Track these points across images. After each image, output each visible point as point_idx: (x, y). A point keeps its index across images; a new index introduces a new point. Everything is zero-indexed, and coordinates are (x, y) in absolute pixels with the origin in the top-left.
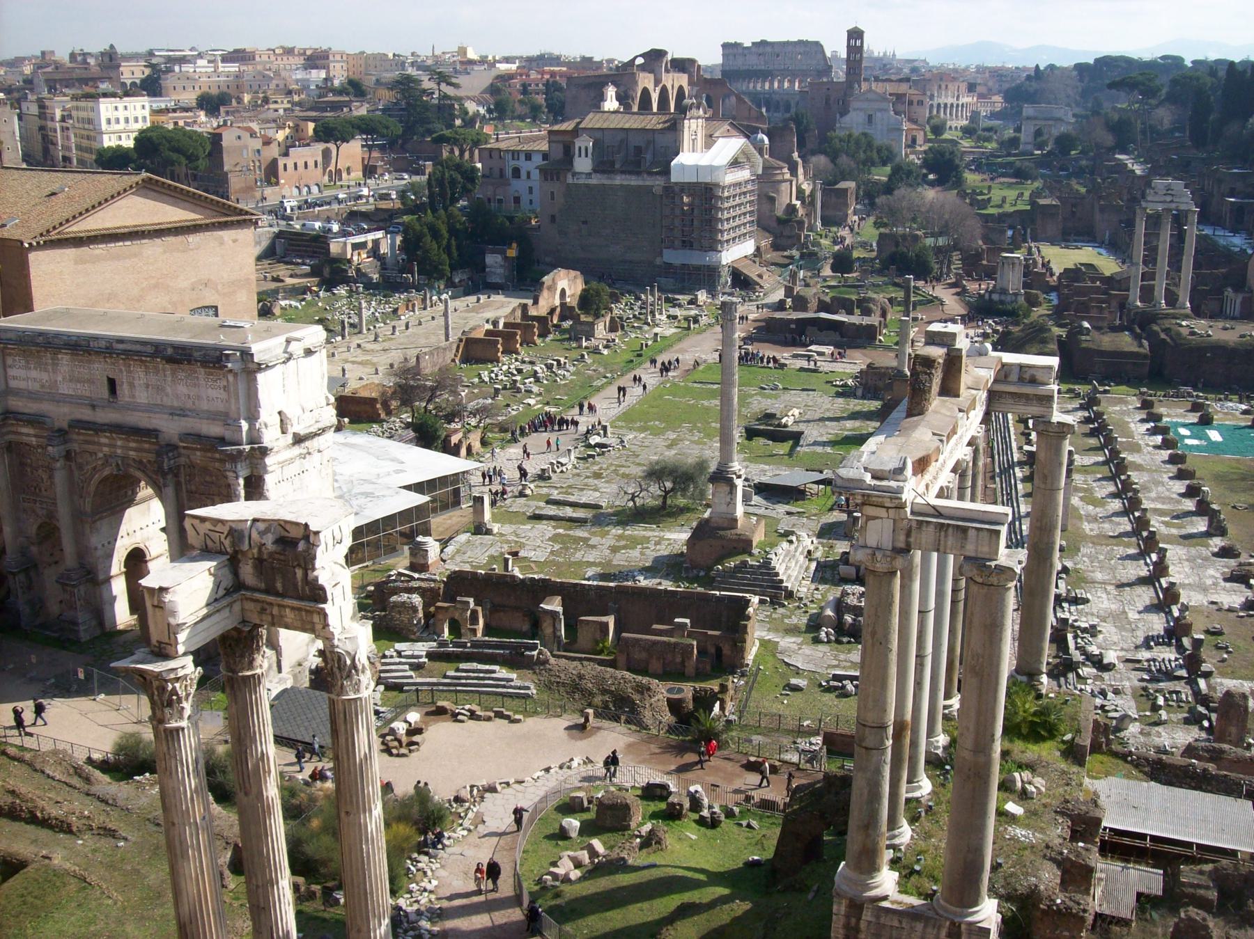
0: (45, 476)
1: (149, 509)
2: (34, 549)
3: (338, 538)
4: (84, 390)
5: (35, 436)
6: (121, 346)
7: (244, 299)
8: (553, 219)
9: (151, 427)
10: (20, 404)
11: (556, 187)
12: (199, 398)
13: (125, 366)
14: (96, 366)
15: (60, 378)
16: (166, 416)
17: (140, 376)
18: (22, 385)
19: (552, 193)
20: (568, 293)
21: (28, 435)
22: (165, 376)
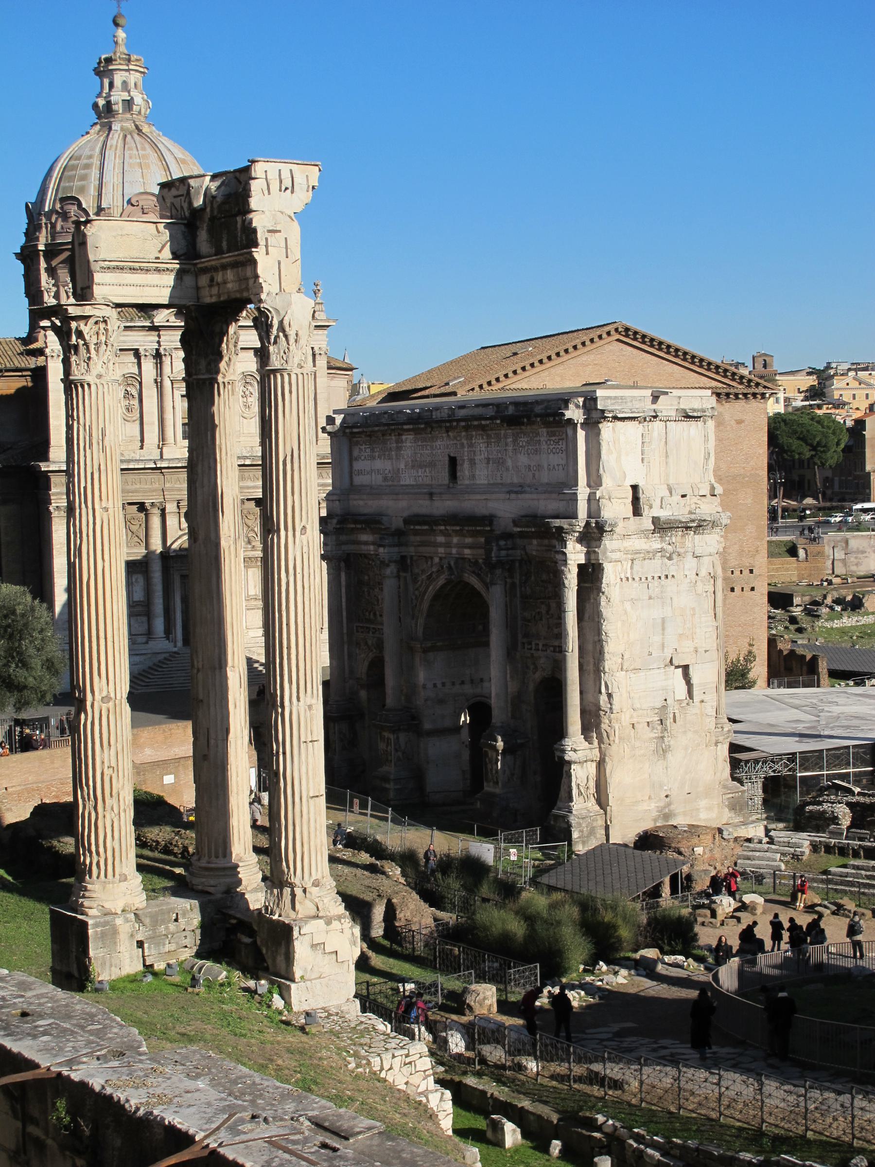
3: (287, 183)
4: (424, 476)
5: (373, 543)
6: (462, 413)
7: (749, 501)
10: (361, 503)
12: (539, 467)
14: (439, 443)
15: (402, 466)
17: (481, 446)
22: (506, 445)
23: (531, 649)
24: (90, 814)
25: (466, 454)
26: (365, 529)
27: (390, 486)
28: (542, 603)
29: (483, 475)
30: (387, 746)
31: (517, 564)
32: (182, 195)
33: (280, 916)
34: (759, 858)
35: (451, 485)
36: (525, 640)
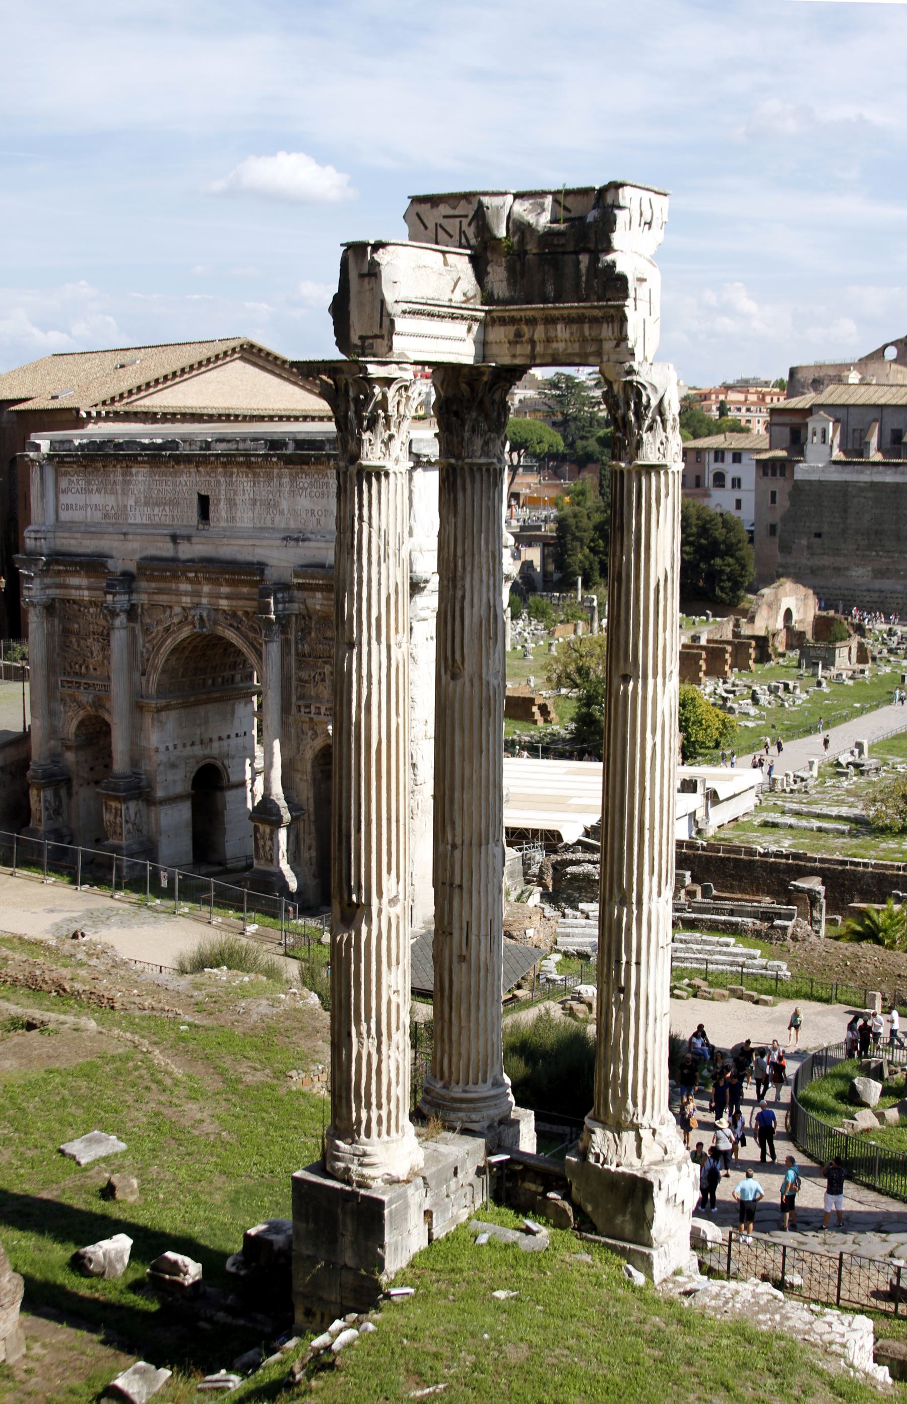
0: (96, 648)
1: (233, 713)
2: (70, 757)
4: (161, 515)
5: (89, 589)
6: (220, 449)
8: (773, 529)
9: (255, 560)
10: (73, 542)
11: (780, 485)
13: (225, 475)
14: (184, 479)
15: (131, 502)
16: (278, 542)
18: (77, 515)
19: (773, 494)
20: (795, 617)
21: (78, 588)
23: (310, 712)
24: (369, 1055)
25: (223, 492)
26: (79, 572)
27: (113, 524)
28: (325, 663)
29: (245, 518)
30: (115, 818)
31: (294, 619)
32: (466, 216)
33: (618, 1166)
34: (578, 935)
35: (201, 526)
36: (301, 703)
